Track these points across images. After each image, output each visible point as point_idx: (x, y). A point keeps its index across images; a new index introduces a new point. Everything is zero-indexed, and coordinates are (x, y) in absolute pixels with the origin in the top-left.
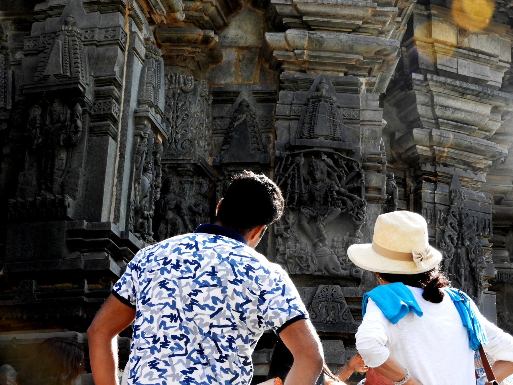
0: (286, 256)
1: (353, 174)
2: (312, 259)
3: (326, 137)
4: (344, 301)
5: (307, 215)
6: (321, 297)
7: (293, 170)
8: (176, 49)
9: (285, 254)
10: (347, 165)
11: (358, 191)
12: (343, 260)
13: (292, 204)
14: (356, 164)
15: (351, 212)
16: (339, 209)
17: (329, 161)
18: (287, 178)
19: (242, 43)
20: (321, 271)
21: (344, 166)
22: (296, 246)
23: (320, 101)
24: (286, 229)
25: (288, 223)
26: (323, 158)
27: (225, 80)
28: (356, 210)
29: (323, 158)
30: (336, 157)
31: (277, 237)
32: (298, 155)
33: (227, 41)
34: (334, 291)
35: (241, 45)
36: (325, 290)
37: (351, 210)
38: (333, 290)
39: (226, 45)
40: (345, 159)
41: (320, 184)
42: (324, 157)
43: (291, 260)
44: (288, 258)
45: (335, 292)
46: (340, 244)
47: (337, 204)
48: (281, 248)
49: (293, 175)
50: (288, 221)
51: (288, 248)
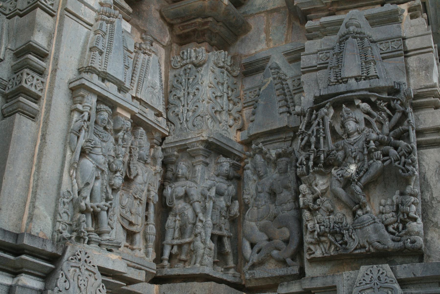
1: (397, 116)
4: (397, 286)
7: (318, 124)
8: (188, 25)
9: (315, 231)
10: (389, 106)
11: (404, 135)
12: (394, 228)
13: (317, 166)
14: (399, 102)
15: (396, 163)
16: (380, 162)
17: (365, 106)
18: (310, 136)
21: (385, 108)
23: (347, 39)
24: (315, 200)
25: (316, 191)
26: (357, 104)
27: (255, 49)
29: (357, 104)
30: (373, 99)
32: (324, 106)
33: (254, 8)
34: (380, 272)
35: (269, 9)
36: (369, 273)
37: (395, 161)
38: (379, 271)
39: (254, 12)
40: (384, 100)
41: (356, 136)
42: (358, 102)
43: (323, 239)
44: (318, 235)
46: (388, 208)
47: (375, 156)
48: (310, 225)
49: (318, 131)
50: (315, 188)
51: (318, 223)
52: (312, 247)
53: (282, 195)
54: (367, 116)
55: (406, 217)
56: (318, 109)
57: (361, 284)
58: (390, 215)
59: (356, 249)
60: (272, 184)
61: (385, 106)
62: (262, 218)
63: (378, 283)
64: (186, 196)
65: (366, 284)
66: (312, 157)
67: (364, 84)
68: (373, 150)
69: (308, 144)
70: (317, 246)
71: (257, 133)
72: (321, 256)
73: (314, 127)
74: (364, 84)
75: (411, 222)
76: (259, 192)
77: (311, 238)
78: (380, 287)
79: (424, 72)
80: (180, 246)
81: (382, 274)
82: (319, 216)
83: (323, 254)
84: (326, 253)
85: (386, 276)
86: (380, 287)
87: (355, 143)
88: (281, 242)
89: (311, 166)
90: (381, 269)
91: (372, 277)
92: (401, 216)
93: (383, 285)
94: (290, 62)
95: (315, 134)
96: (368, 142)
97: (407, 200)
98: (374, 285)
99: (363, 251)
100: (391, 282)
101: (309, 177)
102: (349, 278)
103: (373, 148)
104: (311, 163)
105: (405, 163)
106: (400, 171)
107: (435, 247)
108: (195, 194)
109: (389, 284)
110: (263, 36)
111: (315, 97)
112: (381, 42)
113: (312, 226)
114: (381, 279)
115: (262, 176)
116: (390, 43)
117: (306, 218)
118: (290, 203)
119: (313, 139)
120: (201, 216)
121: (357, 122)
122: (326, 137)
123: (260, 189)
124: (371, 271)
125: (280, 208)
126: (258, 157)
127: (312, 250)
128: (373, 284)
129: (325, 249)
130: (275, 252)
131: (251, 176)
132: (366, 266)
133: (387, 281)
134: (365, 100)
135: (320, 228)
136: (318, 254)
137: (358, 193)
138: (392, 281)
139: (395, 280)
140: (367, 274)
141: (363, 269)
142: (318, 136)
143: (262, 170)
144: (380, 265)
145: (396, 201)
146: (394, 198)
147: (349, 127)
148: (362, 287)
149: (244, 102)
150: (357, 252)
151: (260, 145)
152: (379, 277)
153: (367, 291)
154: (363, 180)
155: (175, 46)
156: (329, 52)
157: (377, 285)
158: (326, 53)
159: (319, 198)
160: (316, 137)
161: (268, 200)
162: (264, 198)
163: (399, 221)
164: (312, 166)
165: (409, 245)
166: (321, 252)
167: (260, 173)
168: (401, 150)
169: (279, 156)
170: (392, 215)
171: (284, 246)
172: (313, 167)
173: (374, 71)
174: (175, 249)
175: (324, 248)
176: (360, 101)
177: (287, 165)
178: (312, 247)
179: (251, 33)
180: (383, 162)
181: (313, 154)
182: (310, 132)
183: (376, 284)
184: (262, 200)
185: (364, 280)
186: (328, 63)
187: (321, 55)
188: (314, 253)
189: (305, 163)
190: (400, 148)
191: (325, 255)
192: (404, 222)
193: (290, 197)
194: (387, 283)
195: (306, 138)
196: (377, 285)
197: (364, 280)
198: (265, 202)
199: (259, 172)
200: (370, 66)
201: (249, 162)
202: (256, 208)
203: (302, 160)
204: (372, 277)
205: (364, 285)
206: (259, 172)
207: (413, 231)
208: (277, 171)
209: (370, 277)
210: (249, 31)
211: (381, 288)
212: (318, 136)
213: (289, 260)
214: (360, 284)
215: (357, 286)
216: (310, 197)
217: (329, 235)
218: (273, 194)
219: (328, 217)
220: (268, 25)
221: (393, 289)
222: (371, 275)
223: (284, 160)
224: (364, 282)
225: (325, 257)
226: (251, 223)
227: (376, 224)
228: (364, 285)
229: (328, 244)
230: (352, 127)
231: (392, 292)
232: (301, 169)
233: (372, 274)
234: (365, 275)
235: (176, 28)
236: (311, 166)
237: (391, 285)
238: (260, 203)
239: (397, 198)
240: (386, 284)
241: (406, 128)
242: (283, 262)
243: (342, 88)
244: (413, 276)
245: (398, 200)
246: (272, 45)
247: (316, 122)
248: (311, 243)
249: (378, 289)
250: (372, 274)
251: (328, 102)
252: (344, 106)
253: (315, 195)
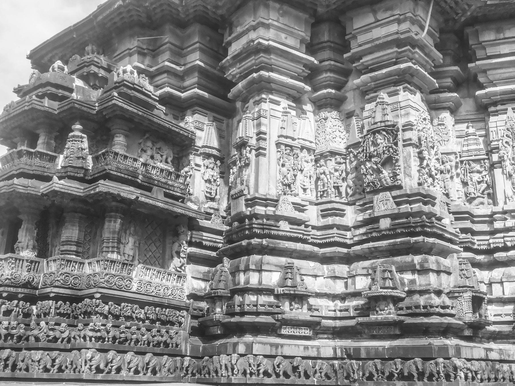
3: (381, 122)
20: (382, 186)
40: (390, 130)
42: (381, 131)
64: (324, 173)
67: (383, 124)
74: (383, 124)
80: (323, 192)
108: (327, 173)
110: (353, 100)
120: (329, 180)
134: (384, 130)
155: (317, 111)
174: (322, 193)
216: (365, 170)
220: (354, 95)
235: (316, 103)
243: (375, 126)
246: (356, 104)
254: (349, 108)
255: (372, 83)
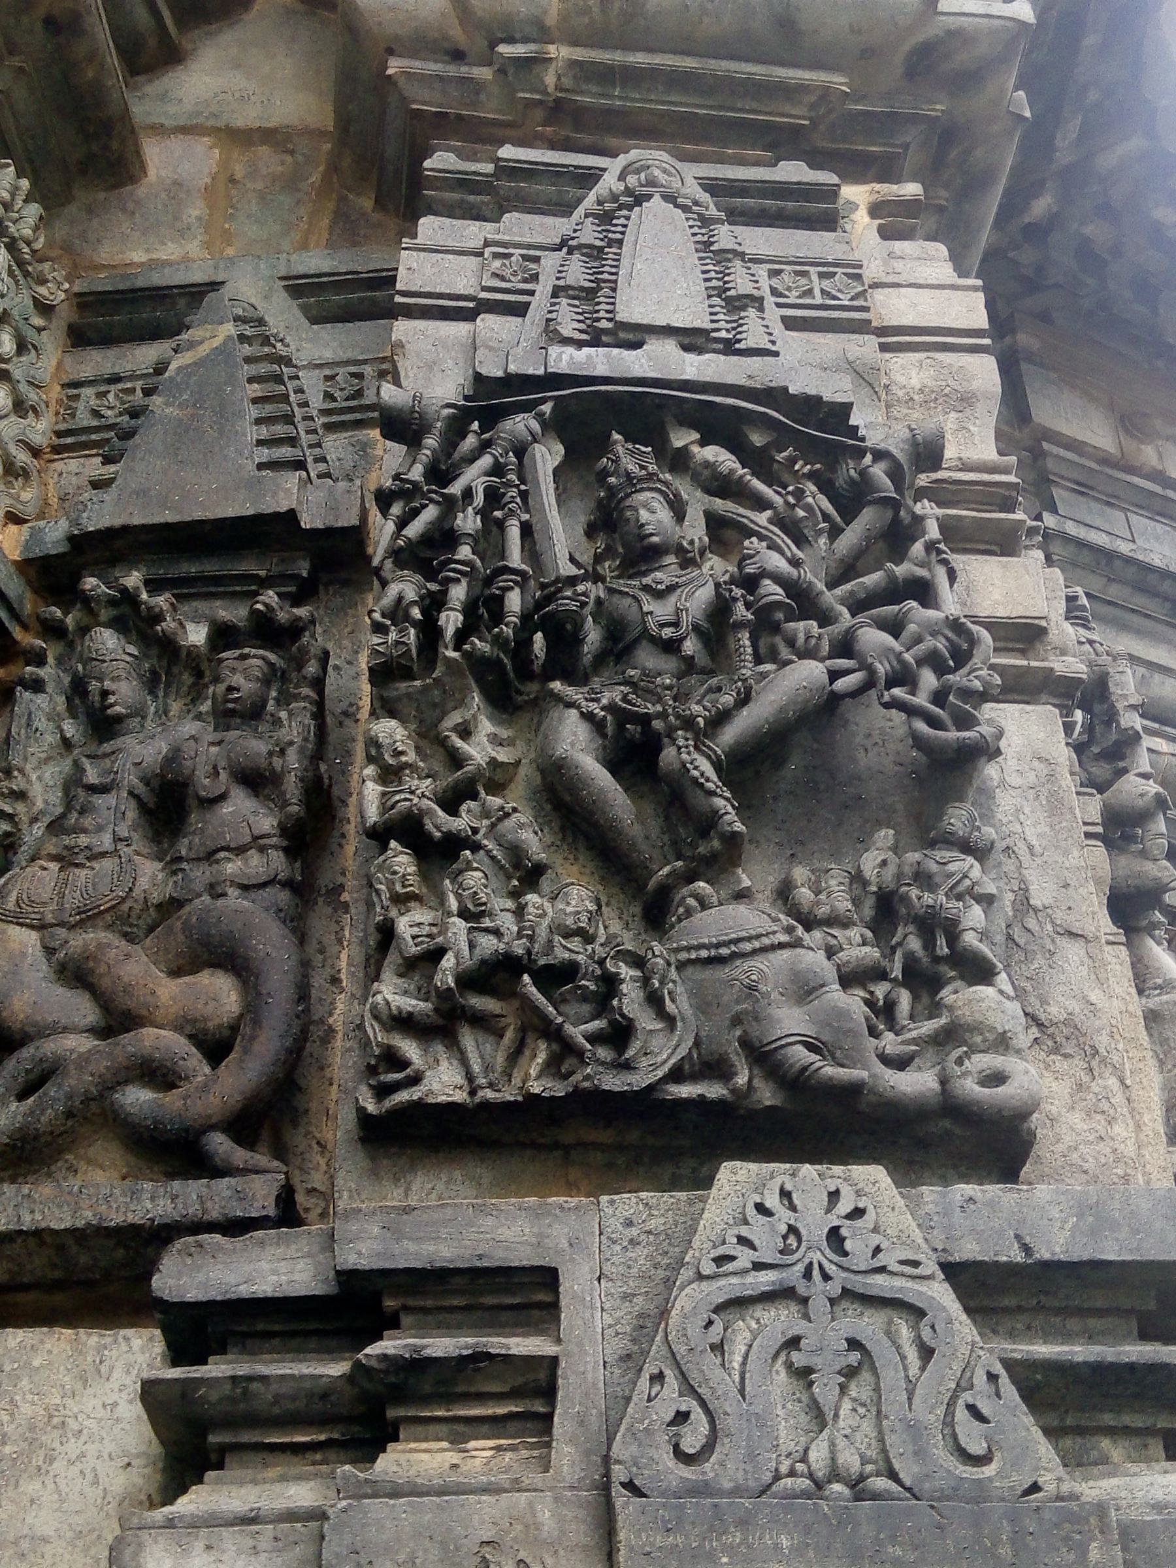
0: (448, 962)
2: (646, 981)
3: (692, 340)
4: (941, 1295)
5: (593, 706)
6: (745, 1257)
18: (450, 506)
19: (247, 117)
20: (716, 1068)
22: (519, 912)
25: (456, 760)
26: (678, 443)
27: (147, 251)
28: (929, 679)
30: (757, 439)
31: (384, 848)
34: (845, 1206)
35: (240, 122)
36: (772, 1201)
37: (891, 683)
38: (834, 1196)
45: (857, 1213)
50: (459, 743)
51: (464, 914)
52: (410, 1049)
53: (226, 809)
54: (720, 505)
55: (943, 949)
56: (491, 417)
57: (730, 1267)
58: (855, 933)
59: (677, 1075)
60: (173, 757)
61: (811, 476)
62: (87, 918)
63: (831, 1269)
65: (758, 1266)
66: (458, 593)
68: (780, 616)
69: (443, 538)
70: (439, 1048)
71: (126, 529)
72: (460, 1097)
73: (474, 476)
75: (959, 983)
76: (93, 789)
77: (405, 993)
78: (846, 1293)
79: (953, 415)
81: (849, 1216)
82: (473, 879)
83: (473, 1093)
84: (491, 1085)
85: (875, 1230)
86: (845, 1291)
87: (671, 589)
88: (183, 1040)
89: (450, 632)
90: (846, 1192)
91: (792, 1230)
92: (914, 944)
93: (860, 1284)
94: (314, 321)
95: (479, 500)
96: (750, 583)
97: (952, 867)
98: (807, 1274)
99: (714, 1091)
100: (908, 1269)
101: (425, 689)
102: (634, 1231)
103: (777, 605)
104: (451, 621)
105: (939, 698)
106: (921, 726)
107: (1060, 1147)
109: (898, 1282)
111: (478, 378)
112: (777, 267)
113: (426, 930)
114: (848, 1245)
115: (119, 719)
116: (815, 278)
117: (390, 884)
118: (262, 850)
119: (468, 522)
121: (678, 510)
122: (537, 527)
123: (92, 776)
124: (785, 1194)
125: (200, 875)
126: (107, 640)
127: (404, 1064)
128: (800, 1268)
129: (487, 1069)
130: (137, 1098)
131: (41, 723)
132: (753, 1166)
133: (888, 1259)
135: (472, 945)
136: (443, 1082)
137: (710, 785)
138: (915, 1264)
139: (930, 1266)
140: (761, 1208)
141: (736, 1178)
142: (498, 514)
143: (125, 692)
144: (837, 1170)
145: (879, 875)
146: (869, 863)
147: (644, 515)
148: (731, 1286)
149: (62, 427)
150: (685, 1091)
151: (133, 579)
152: (834, 1232)
153: (759, 1311)
154: (730, 734)
156: (537, 260)
157: (826, 1277)
158: (525, 258)
159: (474, 797)
160: (484, 513)
161: (135, 836)
162: (114, 819)
163: (897, 972)
164: (458, 631)
165: (970, 1088)
166: (460, 1079)
167: (112, 699)
168: (919, 640)
169: (223, 636)
170: (858, 939)
171: (196, 1063)
172: (461, 637)
173: (767, 337)
175: (482, 1057)
176: (696, 436)
177: (267, 682)
178: (410, 1049)
179: (141, 190)
180: (834, 675)
181: (464, 582)
182: (456, 489)
183: (816, 1272)
184: (100, 829)
185: (743, 1241)
186: (532, 293)
187: (497, 263)
188: (416, 1080)
189: (416, 613)
190: (912, 627)
191: (489, 1094)
192: (923, 981)
193: (267, 823)
194: (882, 1270)
195: (430, 513)
196: (826, 1277)
197: (743, 1241)
198: (117, 839)
199: (105, 694)
200: (743, 314)
201: (50, 660)
202: (54, 866)
203: (400, 599)
204: (792, 1230)
205: (745, 1272)
206: (105, 694)
207: (976, 1028)
208: (206, 707)
209: (783, 1229)
210: (133, 179)
211: (845, 1304)
212: (498, 514)
213: (220, 1144)
214: (721, 1260)
215: (701, 1277)
217: (526, 978)
218: (168, 806)
219: (510, 904)
221: (920, 1313)
222: (784, 1216)
223: (258, 659)
224: (745, 1257)
225: (486, 1105)
226: (14, 931)
227: (798, 950)
228: (745, 1272)
229: (509, 1034)
230: (660, 522)
231: (915, 1327)
232: (393, 636)
233: (793, 1208)
234: (751, 1211)
236: (450, 632)
237: (910, 1284)
238: (83, 840)
239: (884, 863)
240: (879, 1279)
241: (922, 572)
242: (175, 1151)
244: (1020, 1257)
245: (889, 873)
247: (486, 461)
248: (404, 1023)
249: (833, 1301)
250: (793, 1208)
251: (544, 401)
252: (616, 436)
253: (452, 778)
254: (139, 256)
255: (560, 52)
